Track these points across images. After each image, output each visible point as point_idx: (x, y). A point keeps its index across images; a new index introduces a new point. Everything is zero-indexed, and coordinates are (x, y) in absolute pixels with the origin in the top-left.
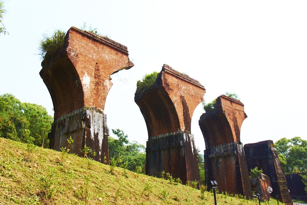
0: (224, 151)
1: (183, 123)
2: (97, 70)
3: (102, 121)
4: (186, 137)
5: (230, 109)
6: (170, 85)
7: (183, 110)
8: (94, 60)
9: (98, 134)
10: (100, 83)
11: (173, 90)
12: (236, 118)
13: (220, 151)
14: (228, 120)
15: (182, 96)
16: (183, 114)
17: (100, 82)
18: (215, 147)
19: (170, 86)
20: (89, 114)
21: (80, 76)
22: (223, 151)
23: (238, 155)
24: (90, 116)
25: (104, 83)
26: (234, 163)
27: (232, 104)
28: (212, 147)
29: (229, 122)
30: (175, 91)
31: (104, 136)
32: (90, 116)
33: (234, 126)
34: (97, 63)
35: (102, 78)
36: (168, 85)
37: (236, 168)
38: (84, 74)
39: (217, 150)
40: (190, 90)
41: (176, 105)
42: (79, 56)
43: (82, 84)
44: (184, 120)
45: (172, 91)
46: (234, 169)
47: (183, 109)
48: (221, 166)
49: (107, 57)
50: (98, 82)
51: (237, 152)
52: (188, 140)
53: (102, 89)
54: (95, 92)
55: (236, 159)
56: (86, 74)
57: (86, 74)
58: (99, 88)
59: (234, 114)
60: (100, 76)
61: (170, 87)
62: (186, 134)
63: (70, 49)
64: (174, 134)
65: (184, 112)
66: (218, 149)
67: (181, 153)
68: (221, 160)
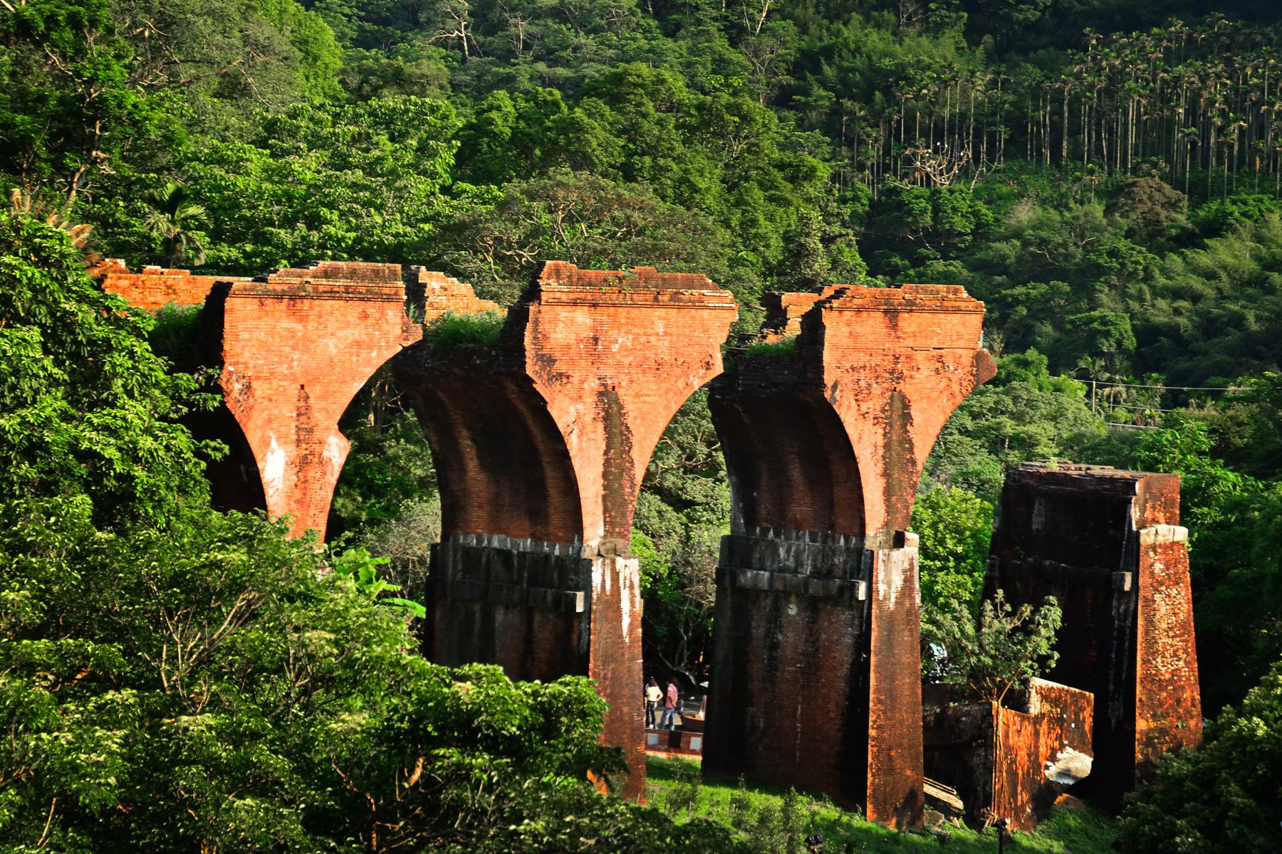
0: (816, 573)
2: (303, 412)
5: (878, 360)
6: (557, 355)
7: (606, 453)
8: (294, 380)
10: (310, 457)
11: (568, 377)
12: (906, 405)
13: (799, 564)
14: (850, 430)
15: (605, 386)
16: (601, 469)
17: (312, 453)
18: (777, 535)
19: (554, 361)
21: (258, 457)
22: (808, 570)
23: (870, 608)
25: (326, 454)
26: (849, 640)
27: (894, 326)
28: (765, 532)
29: (853, 437)
30: (575, 380)
33: (881, 452)
34: (302, 387)
35: (317, 435)
36: (547, 360)
37: (852, 664)
39: (782, 552)
40: (653, 339)
41: (573, 443)
42: (255, 384)
43: (264, 481)
44: (604, 497)
45: (565, 380)
47: (603, 447)
48: (790, 639)
50: (305, 457)
53: (318, 475)
54: (298, 494)
55: (861, 625)
57: (274, 444)
58: (310, 474)
59: (901, 377)
60: (310, 431)
61: (557, 364)
62: (603, 564)
63: (231, 373)
64: (557, 552)
65: (607, 463)
66: (788, 552)
67: (575, 637)
68: (793, 610)
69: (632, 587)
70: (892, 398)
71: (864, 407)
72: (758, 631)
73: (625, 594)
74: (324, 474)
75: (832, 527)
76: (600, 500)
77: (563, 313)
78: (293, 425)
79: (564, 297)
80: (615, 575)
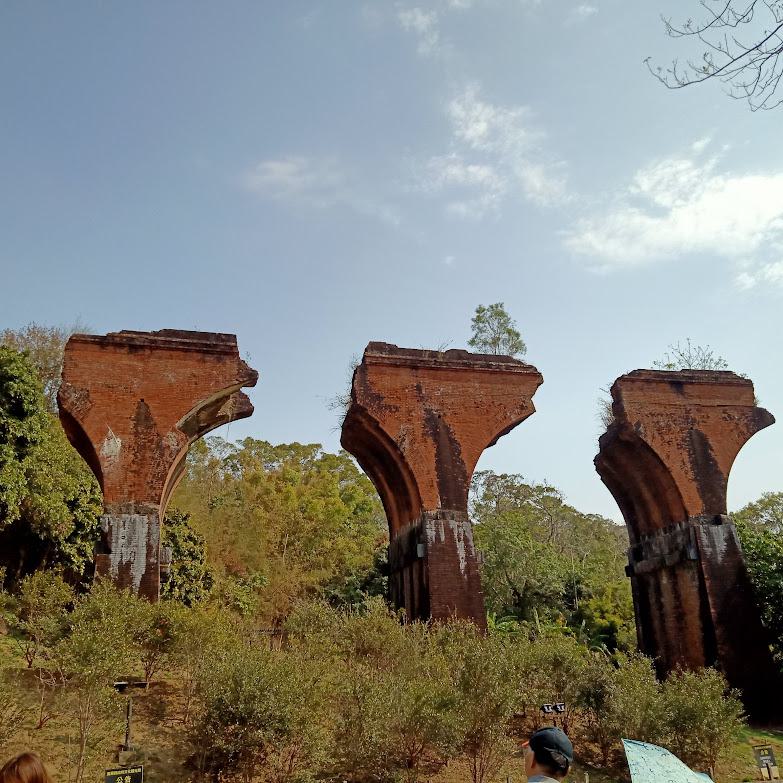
1: (436, 491)
3: (146, 530)
4: (437, 532)
9: (129, 564)
11: (397, 408)
20: (109, 523)
24: (111, 527)
29: (663, 456)
31: (149, 566)
32: (111, 527)
38: (103, 433)
46: (697, 613)
49: (171, 377)
51: (698, 552)
52: (443, 538)
56: (110, 433)
57: (110, 433)
58: (148, 454)
69: (466, 540)
70: (690, 433)
71: (667, 438)
72: (652, 600)
73: (460, 546)
74: (162, 455)
75: (672, 519)
76: (435, 485)
77: (389, 370)
78: (132, 423)
79: (386, 361)
80: (449, 532)
